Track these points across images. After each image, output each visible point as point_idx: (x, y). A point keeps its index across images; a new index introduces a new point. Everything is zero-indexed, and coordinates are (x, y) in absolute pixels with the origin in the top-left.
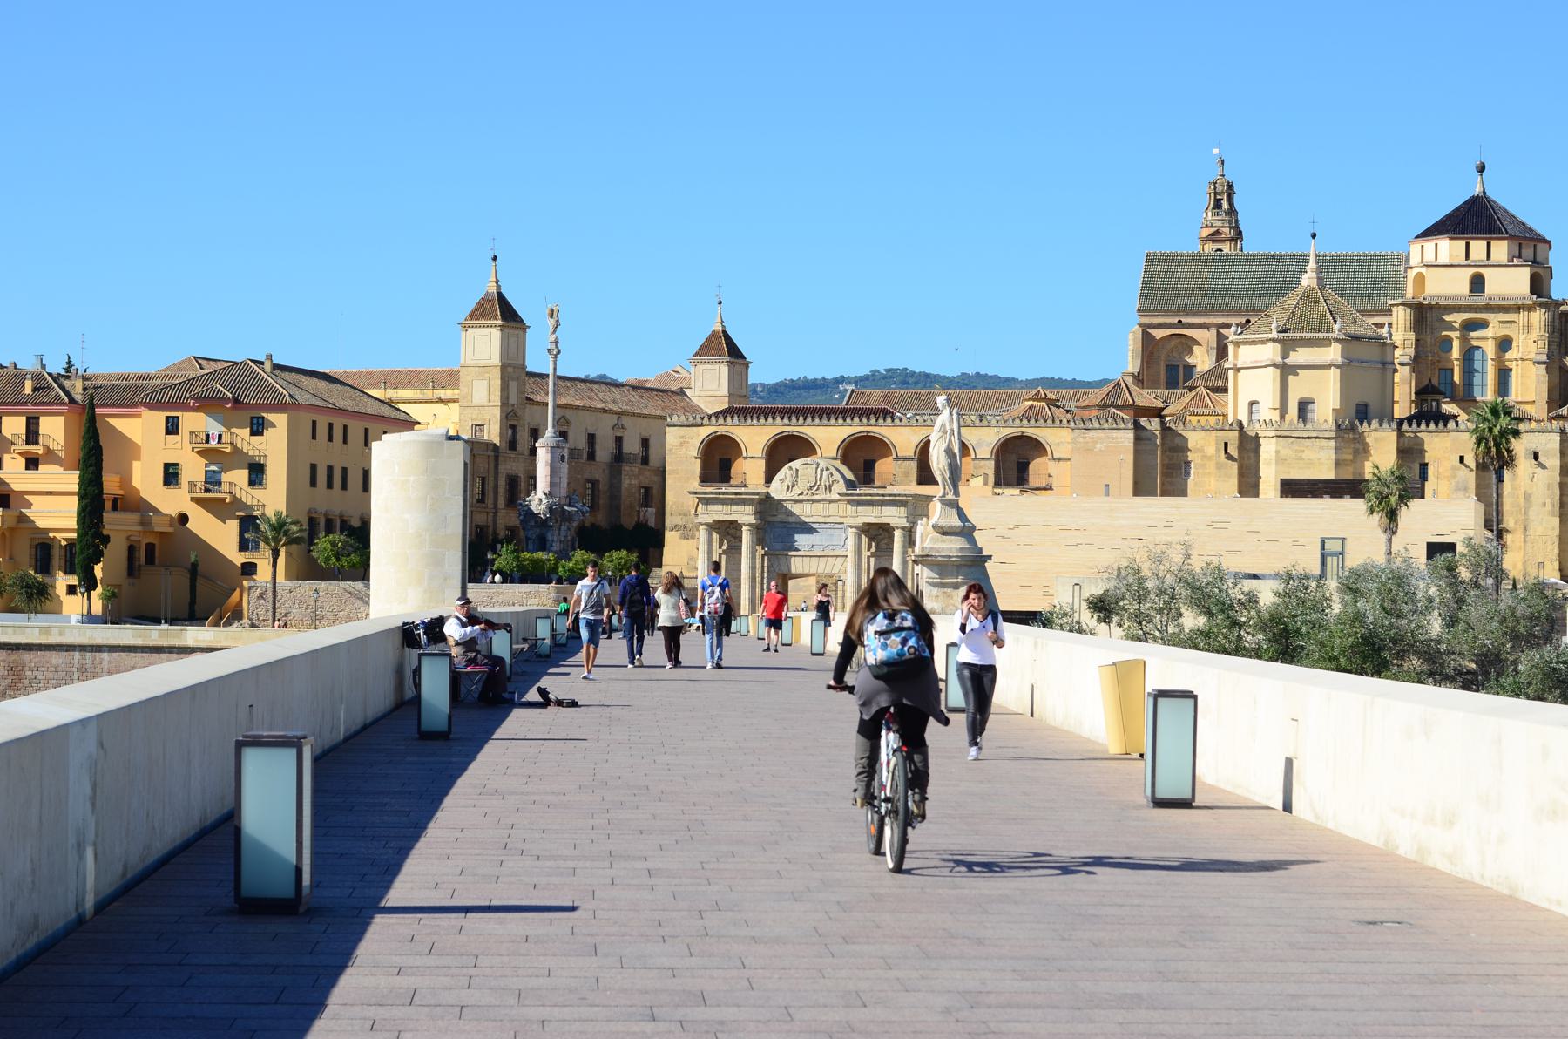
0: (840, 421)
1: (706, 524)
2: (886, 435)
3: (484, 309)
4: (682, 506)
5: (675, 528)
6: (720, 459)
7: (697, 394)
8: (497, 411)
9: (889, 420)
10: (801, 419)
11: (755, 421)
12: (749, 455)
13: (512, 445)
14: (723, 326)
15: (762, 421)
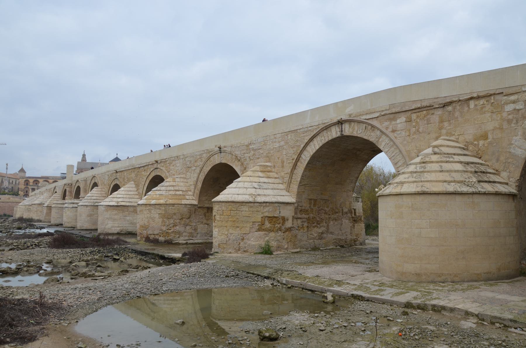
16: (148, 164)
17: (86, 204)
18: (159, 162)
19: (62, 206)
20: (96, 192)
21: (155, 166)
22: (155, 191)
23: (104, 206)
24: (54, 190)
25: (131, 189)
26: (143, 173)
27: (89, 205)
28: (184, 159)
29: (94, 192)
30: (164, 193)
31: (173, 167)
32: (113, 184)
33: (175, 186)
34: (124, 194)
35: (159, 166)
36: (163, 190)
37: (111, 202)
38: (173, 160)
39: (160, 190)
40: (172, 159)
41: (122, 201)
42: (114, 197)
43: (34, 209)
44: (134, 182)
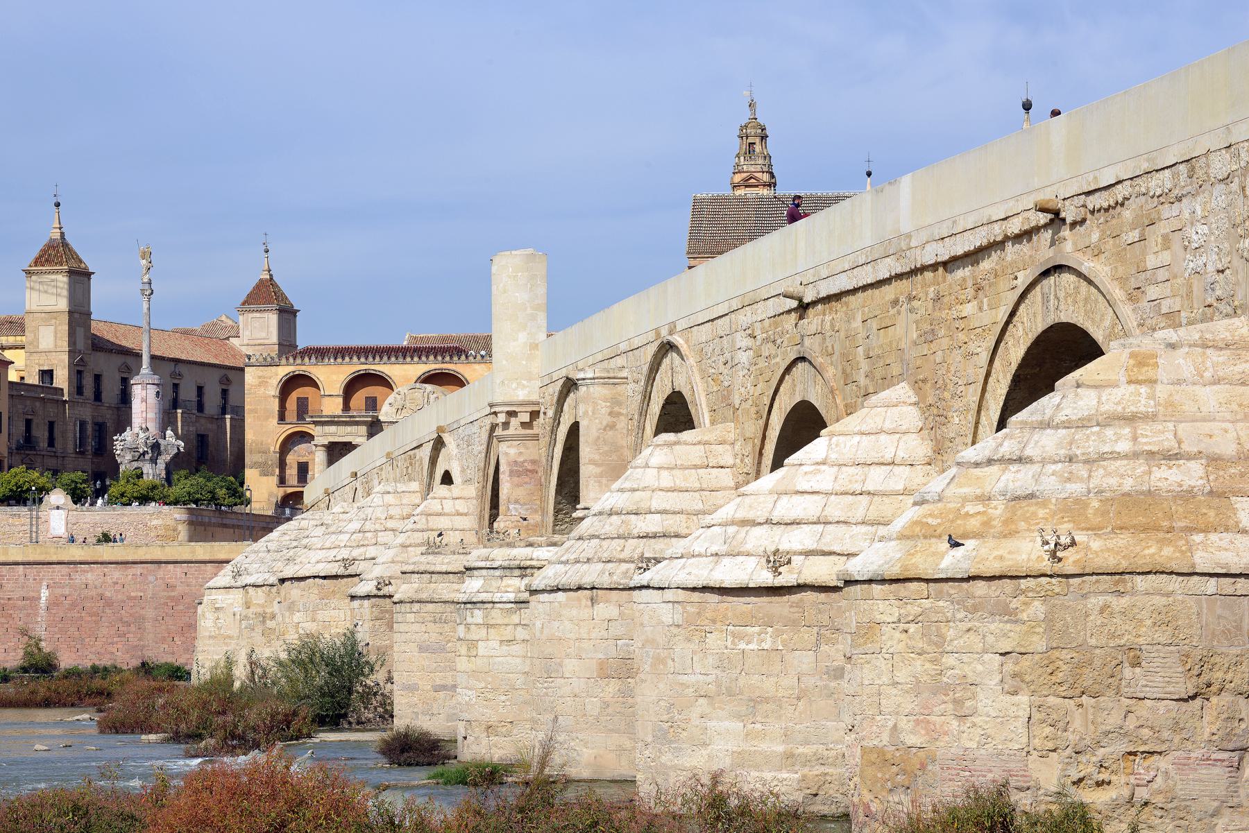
0: (416, 359)
1: (323, 446)
2: (462, 372)
3: (49, 255)
4: (262, 444)
5: (255, 465)
6: (298, 398)
7: (245, 342)
8: (65, 357)
9: (463, 357)
10: (378, 358)
11: (332, 360)
12: (326, 394)
13: (79, 390)
14: (271, 275)
15: (339, 360)
16: (997, 232)
17: (590, 574)
18: (1069, 214)
19: (445, 590)
20: (666, 480)
21: (1041, 251)
22: (977, 465)
23: (669, 595)
24: (433, 461)
25: (887, 447)
26: (968, 309)
27: (606, 581)
28: (1235, 186)
29: (649, 477)
30: (1050, 483)
31: (1166, 257)
32: (785, 403)
33: (1150, 418)
34: (826, 485)
35: (1068, 247)
36: (1044, 462)
37: (726, 561)
38: (1165, 198)
39: (1020, 460)
40: (1156, 184)
41: (810, 545)
42: (750, 515)
43: (297, 617)
44: (918, 385)
